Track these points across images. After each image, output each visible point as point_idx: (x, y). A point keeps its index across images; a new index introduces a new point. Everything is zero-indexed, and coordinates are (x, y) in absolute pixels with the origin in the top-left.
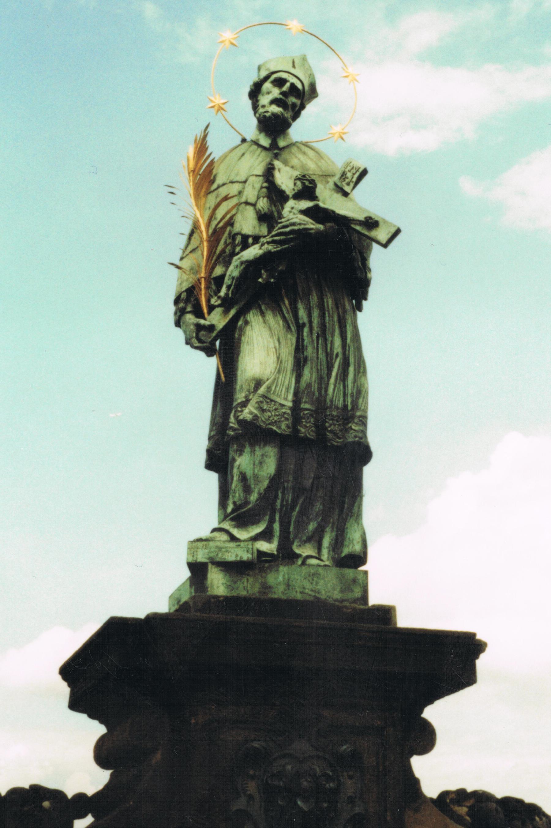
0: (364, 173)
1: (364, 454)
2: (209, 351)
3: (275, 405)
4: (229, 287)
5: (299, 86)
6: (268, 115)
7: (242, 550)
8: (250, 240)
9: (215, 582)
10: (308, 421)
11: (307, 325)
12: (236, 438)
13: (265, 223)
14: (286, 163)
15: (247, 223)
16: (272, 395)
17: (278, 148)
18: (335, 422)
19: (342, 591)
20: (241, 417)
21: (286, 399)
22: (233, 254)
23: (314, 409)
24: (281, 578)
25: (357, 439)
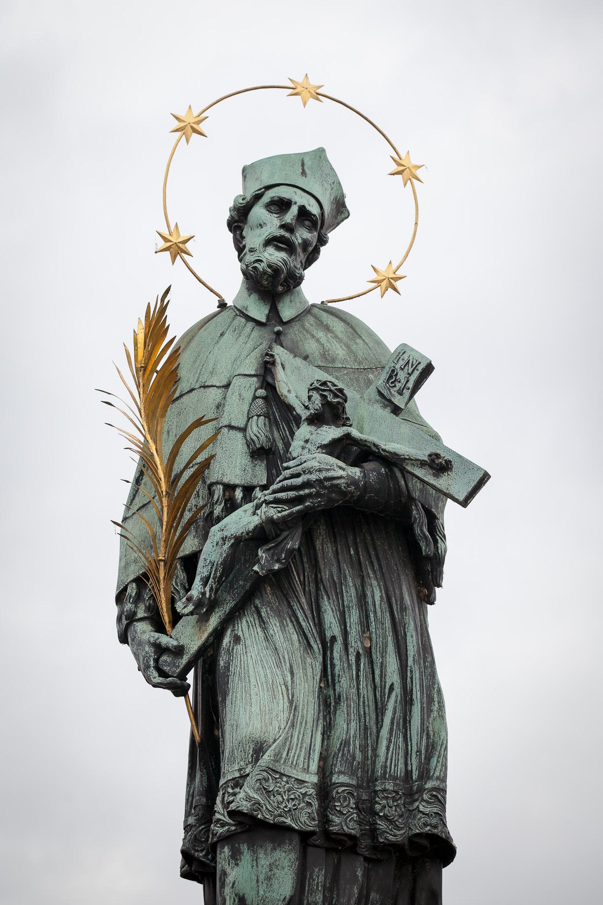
0: (429, 369)
1: (442, 851)
2: (180, 690)
3: (287, 782)
4: (205, 581)
5: (314, 209)
6: (261, 267)
10: (346, 803)
11: (340, 640)
12: (226, 839)
13: (262, 461)
14: (294, 351)
15: (233, 465)
16: (283, 766)
17: (281, 322)
20: (233, 806)
21: (306, 770)
22: (211, 520)
23: (354, 783)
25: (429, 828)
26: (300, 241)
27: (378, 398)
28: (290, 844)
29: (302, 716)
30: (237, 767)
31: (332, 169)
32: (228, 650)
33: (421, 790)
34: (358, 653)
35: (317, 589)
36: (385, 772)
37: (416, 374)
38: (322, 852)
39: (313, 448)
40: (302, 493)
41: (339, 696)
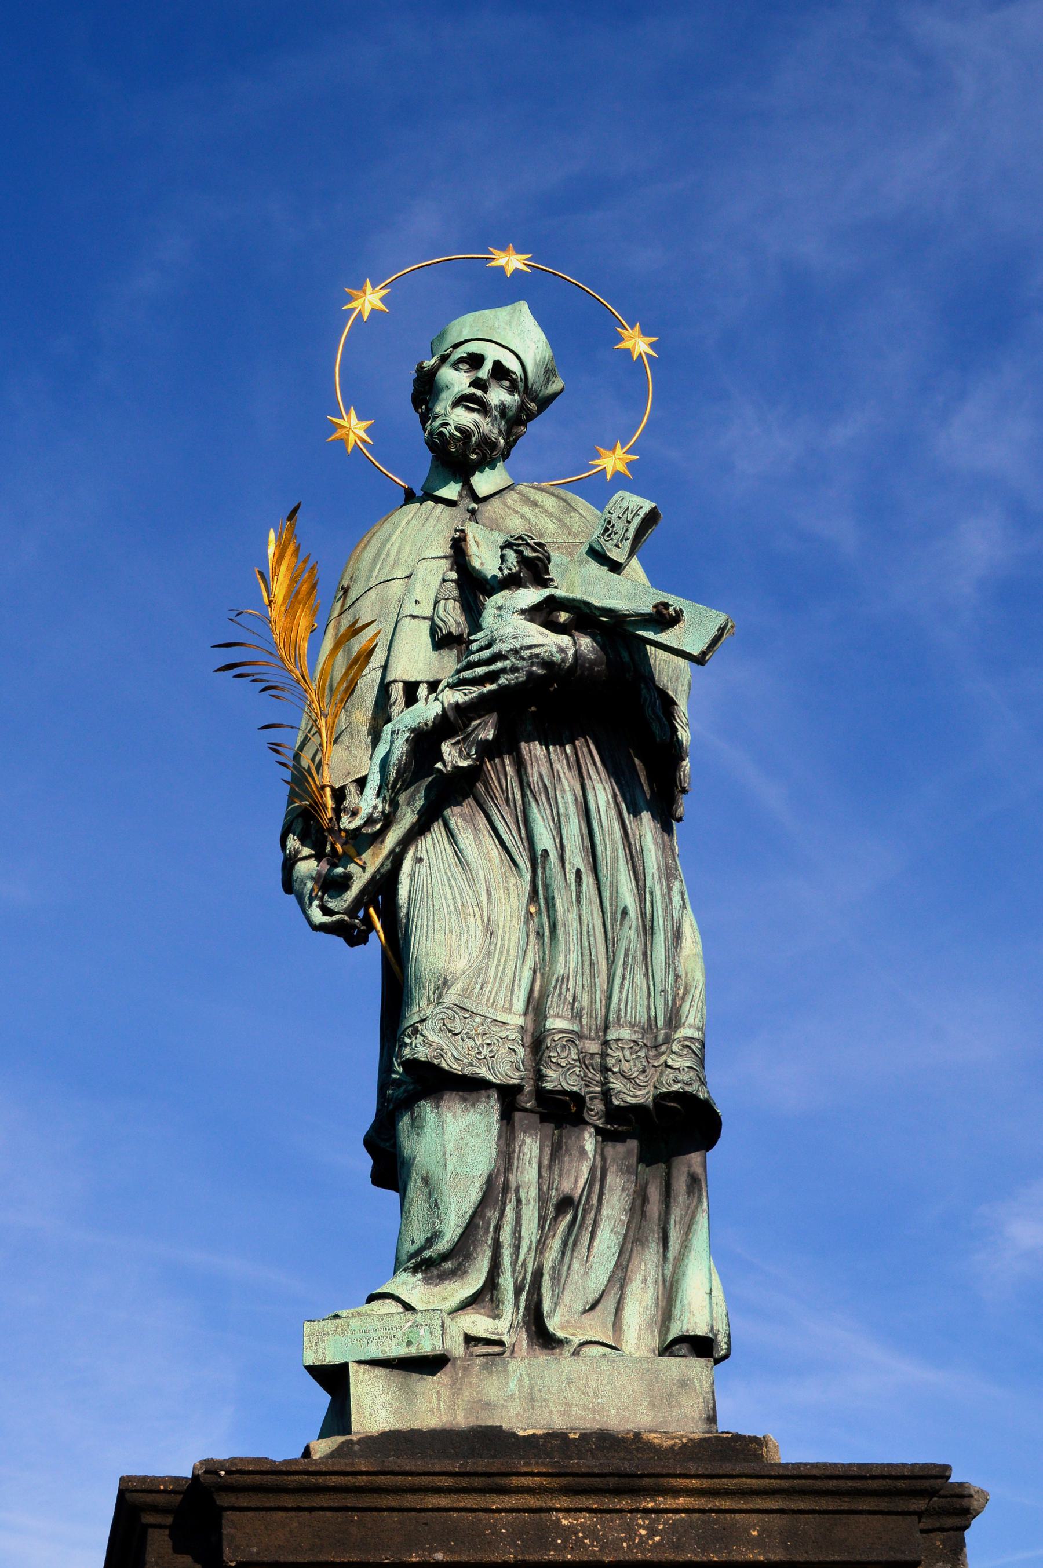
8: (423, 691)
9: (367, 1402)
15: (415, 658)
17: (476, 499)
18: (627, 1053)
19: (653, 1405)
21: (510, 1010)
23: (575, 1028)
24: (513, 1386)
25: (679, 1085)
29: (502, 944)
33: (668, 1040)
34: (578, 871)
36: (618, 1017)
37: (637, 521)
38: (536, 1118)
40: (493, 667)
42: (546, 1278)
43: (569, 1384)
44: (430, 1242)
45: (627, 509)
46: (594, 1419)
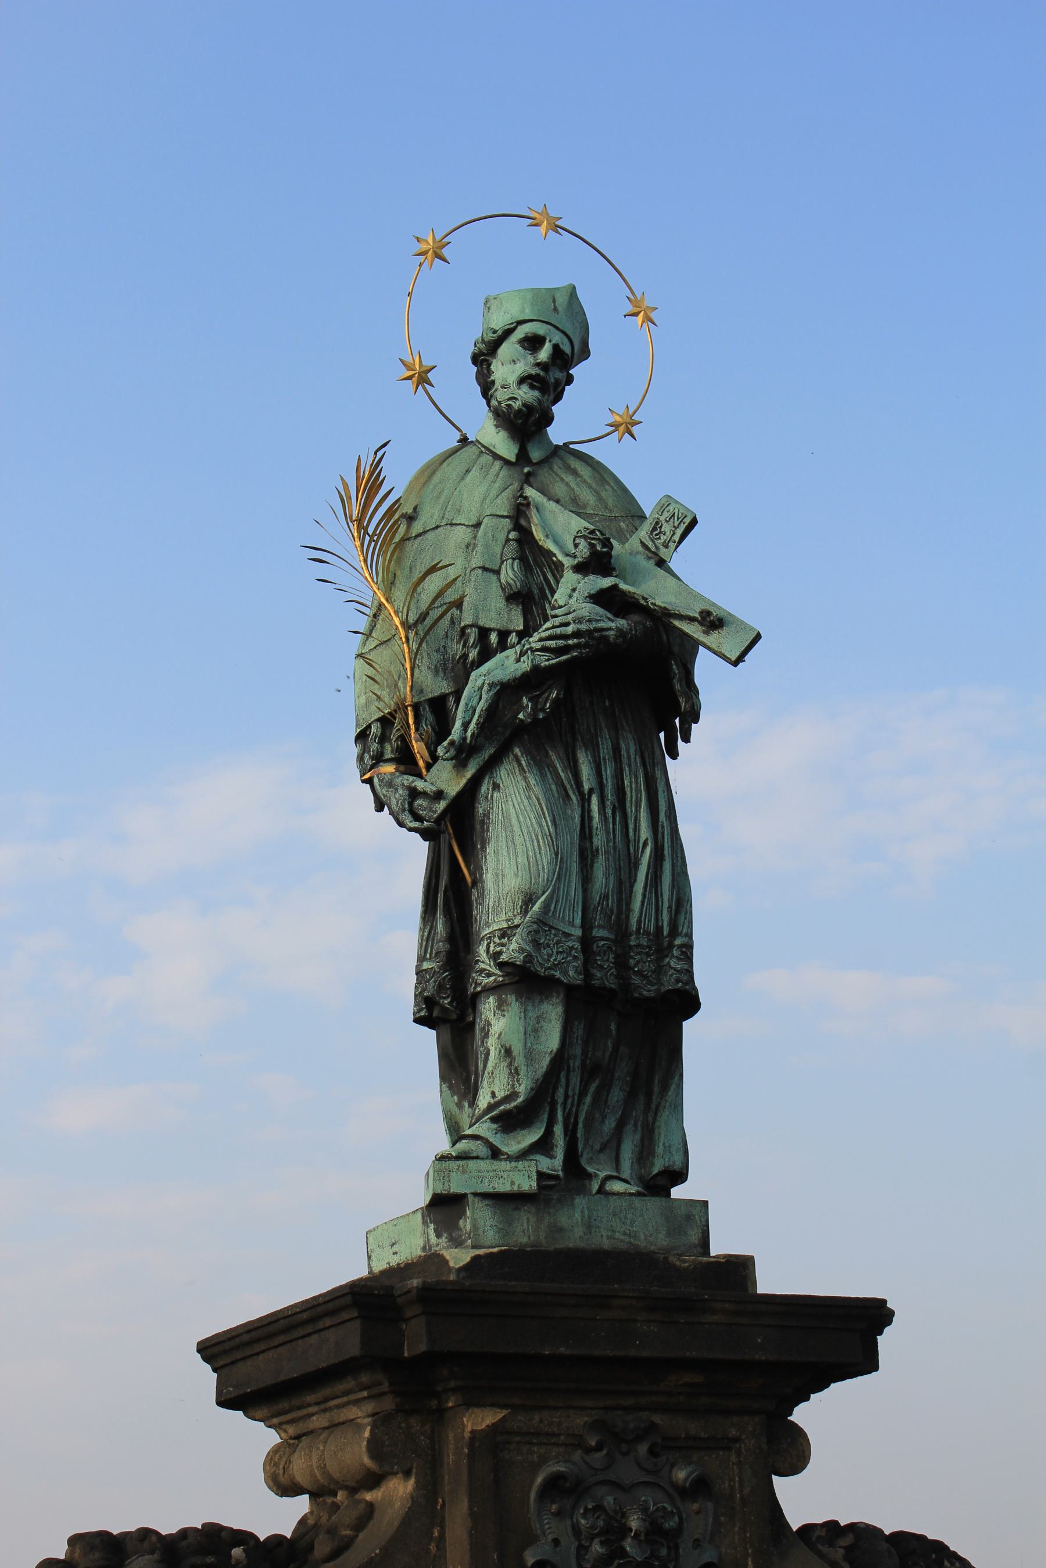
3: (555, 935)
5: (566, 348)
7: (521, 1173)
8: (493, 638)
9: (481, 1222)
10: (605, 958)
11: (597, 791)
13: (517, 605)
19: (669, 1234)
20: (504, 957)
21: (572, 924)
23: (612, 937)
24: (578, 1215)
26: (553, 380)
27: (641, 549)
28: (558, 997)
30: (504, 917)
31: (582, 307)
32: (487, 797)
33: (671, 946)
35: (574, 740)
37: (683, 527)
39: (581, 598)
40: (570, 642)
41: (597, 850)
42: (580, 1125)
43: (614, 1215)
44: (507, 1099)
45: (673, 515)
46: (630, 1242)
